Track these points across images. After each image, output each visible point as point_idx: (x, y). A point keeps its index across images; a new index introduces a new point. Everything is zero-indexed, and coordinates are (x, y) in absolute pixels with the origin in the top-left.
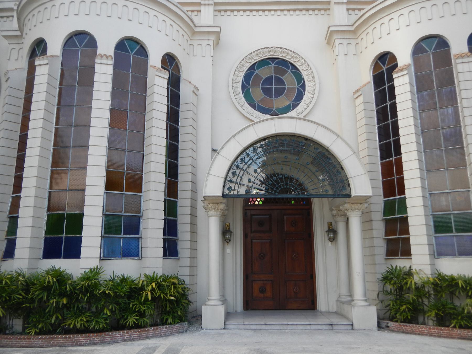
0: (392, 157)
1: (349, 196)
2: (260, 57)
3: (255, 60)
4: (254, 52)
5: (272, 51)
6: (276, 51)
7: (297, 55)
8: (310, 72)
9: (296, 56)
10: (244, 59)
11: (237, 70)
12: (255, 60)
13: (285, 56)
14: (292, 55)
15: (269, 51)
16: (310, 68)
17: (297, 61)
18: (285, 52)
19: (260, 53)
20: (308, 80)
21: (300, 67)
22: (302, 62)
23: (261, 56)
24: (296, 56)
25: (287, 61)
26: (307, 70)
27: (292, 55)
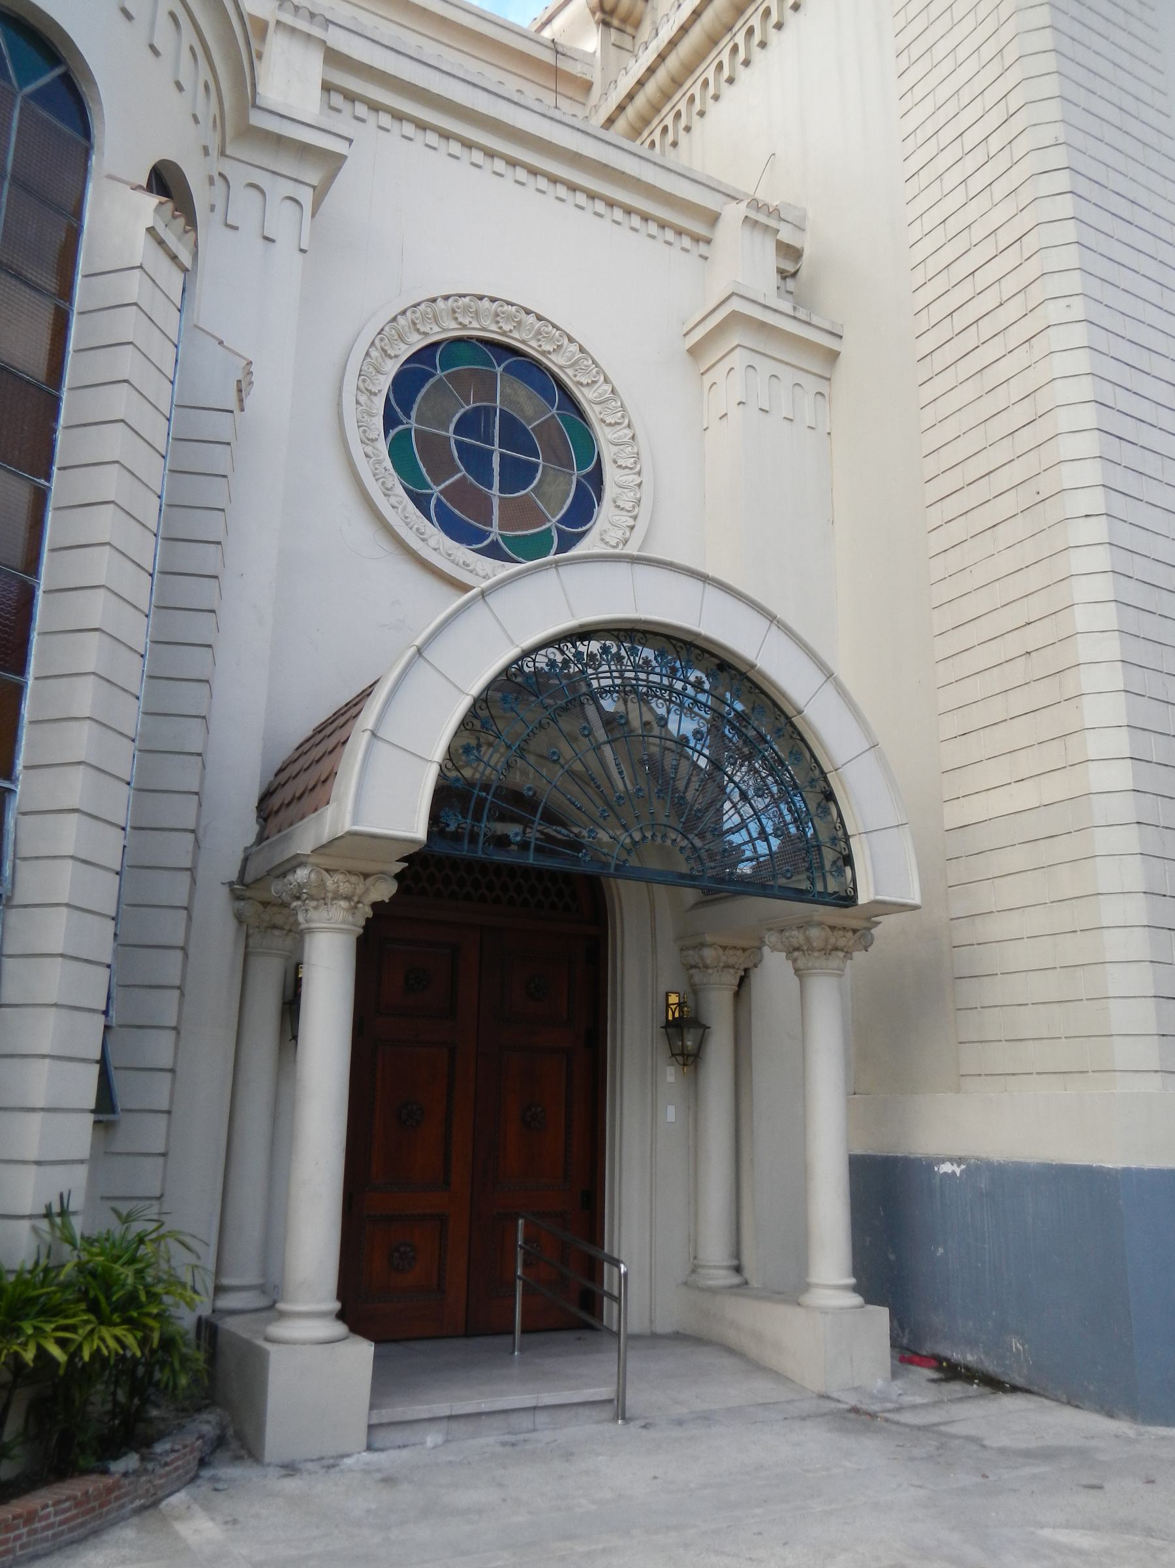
0: (493, 796)
1: (848, 899)
2: (460, 324)
3: (444, 330)
4: (446, 298)
5: (509, 318)
6: (519, 323)
7: (590, 362)
8: (626, 435)
9: (585, 362)
10: (409, 313)
11: (377, 342)
12: (444, 330)
13: (549, 352)
14: (574, 355)
15: (497, 315)
16: (626, 421)
17: (585, 382)
18: (550, 339)
19: (466, 310)
20: (615, 462)
21: (594, 411)
22: (605, 391)
23: (466, 321)
24: (585, 362)
25: (548, 369)
26: (617, 424)
27: (574, 355)
